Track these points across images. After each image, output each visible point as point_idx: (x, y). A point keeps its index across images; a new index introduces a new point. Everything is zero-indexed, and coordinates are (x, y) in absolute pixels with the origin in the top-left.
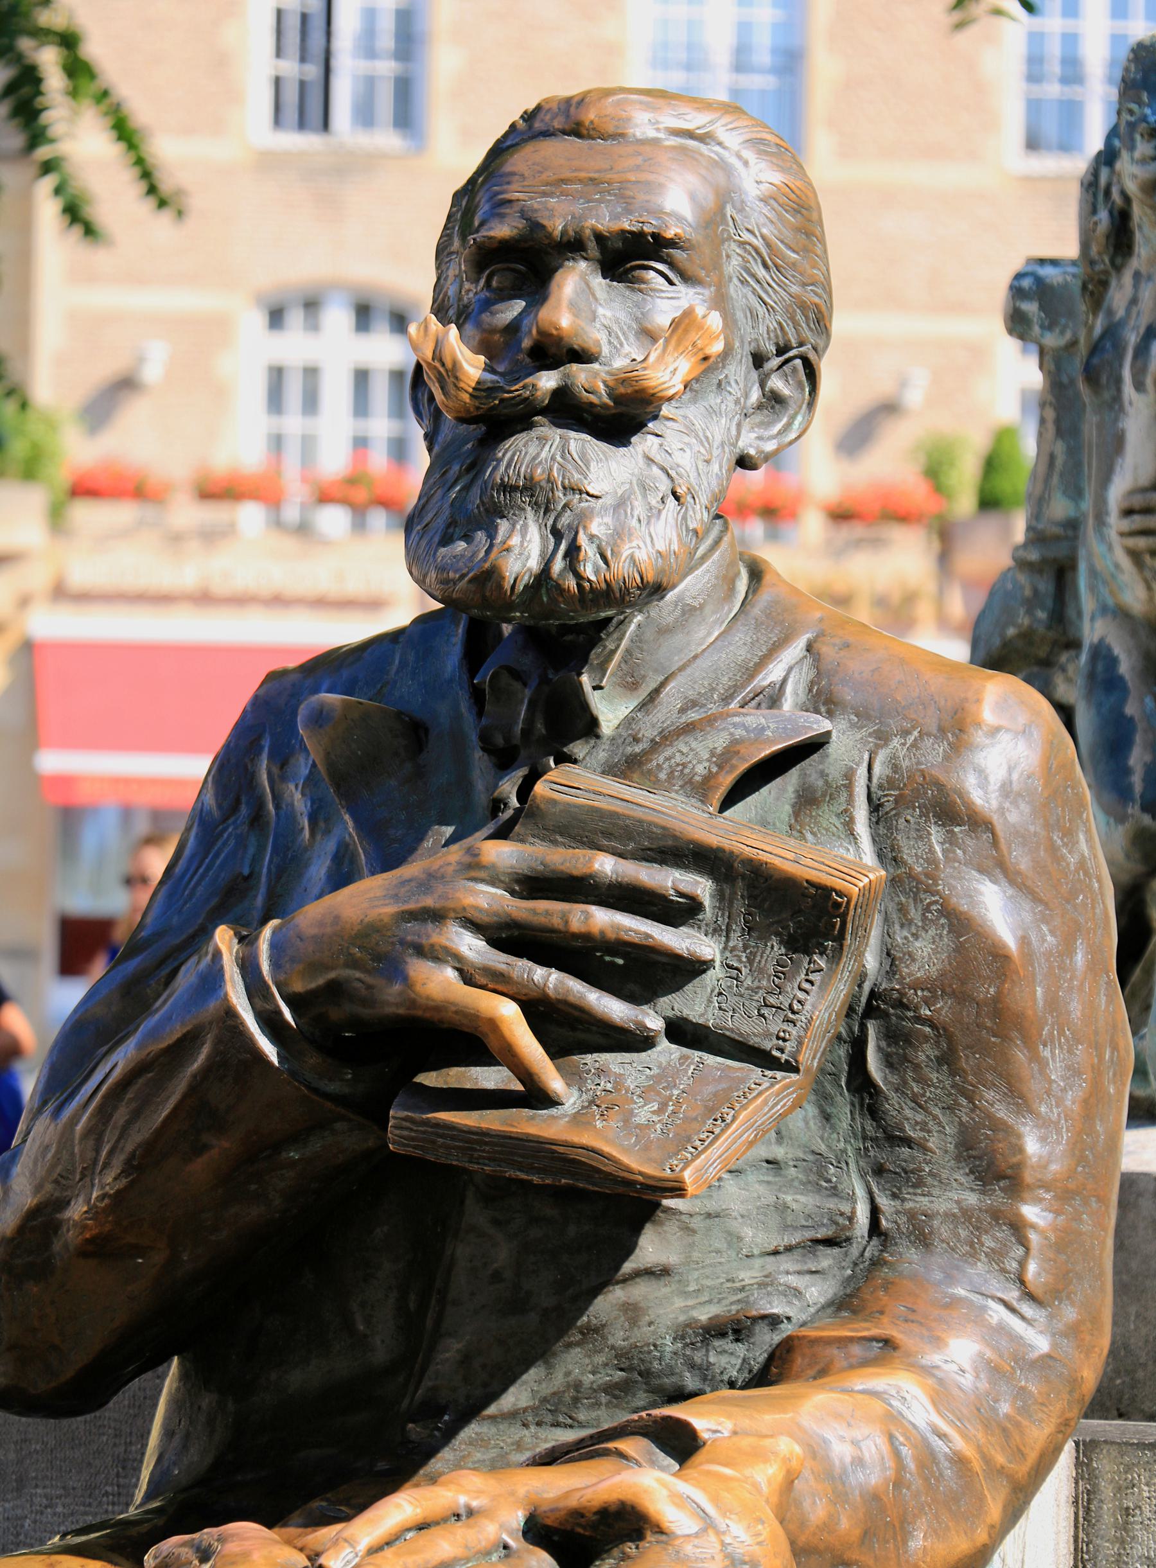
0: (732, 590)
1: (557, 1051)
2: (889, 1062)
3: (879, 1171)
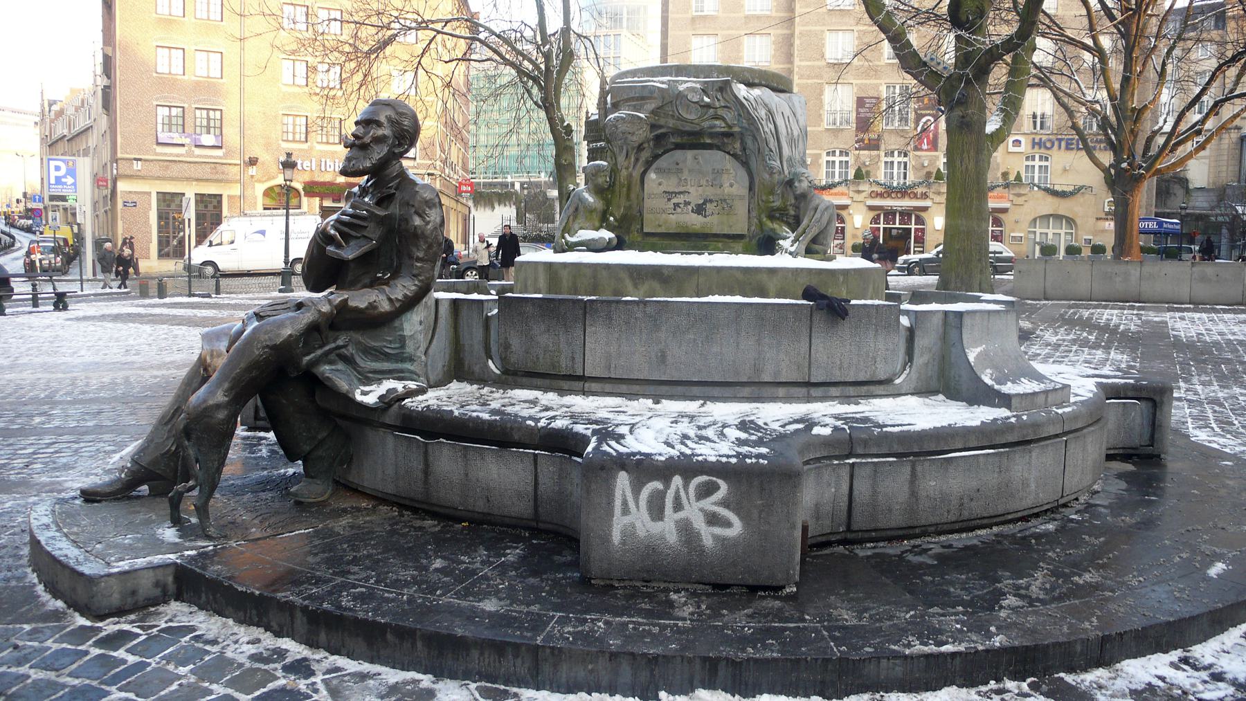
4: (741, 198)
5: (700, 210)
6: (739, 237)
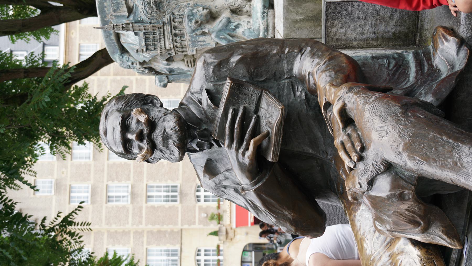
0: (184, 108)
1: (260, 133)
2: (261, 77)
3: (280, 78)
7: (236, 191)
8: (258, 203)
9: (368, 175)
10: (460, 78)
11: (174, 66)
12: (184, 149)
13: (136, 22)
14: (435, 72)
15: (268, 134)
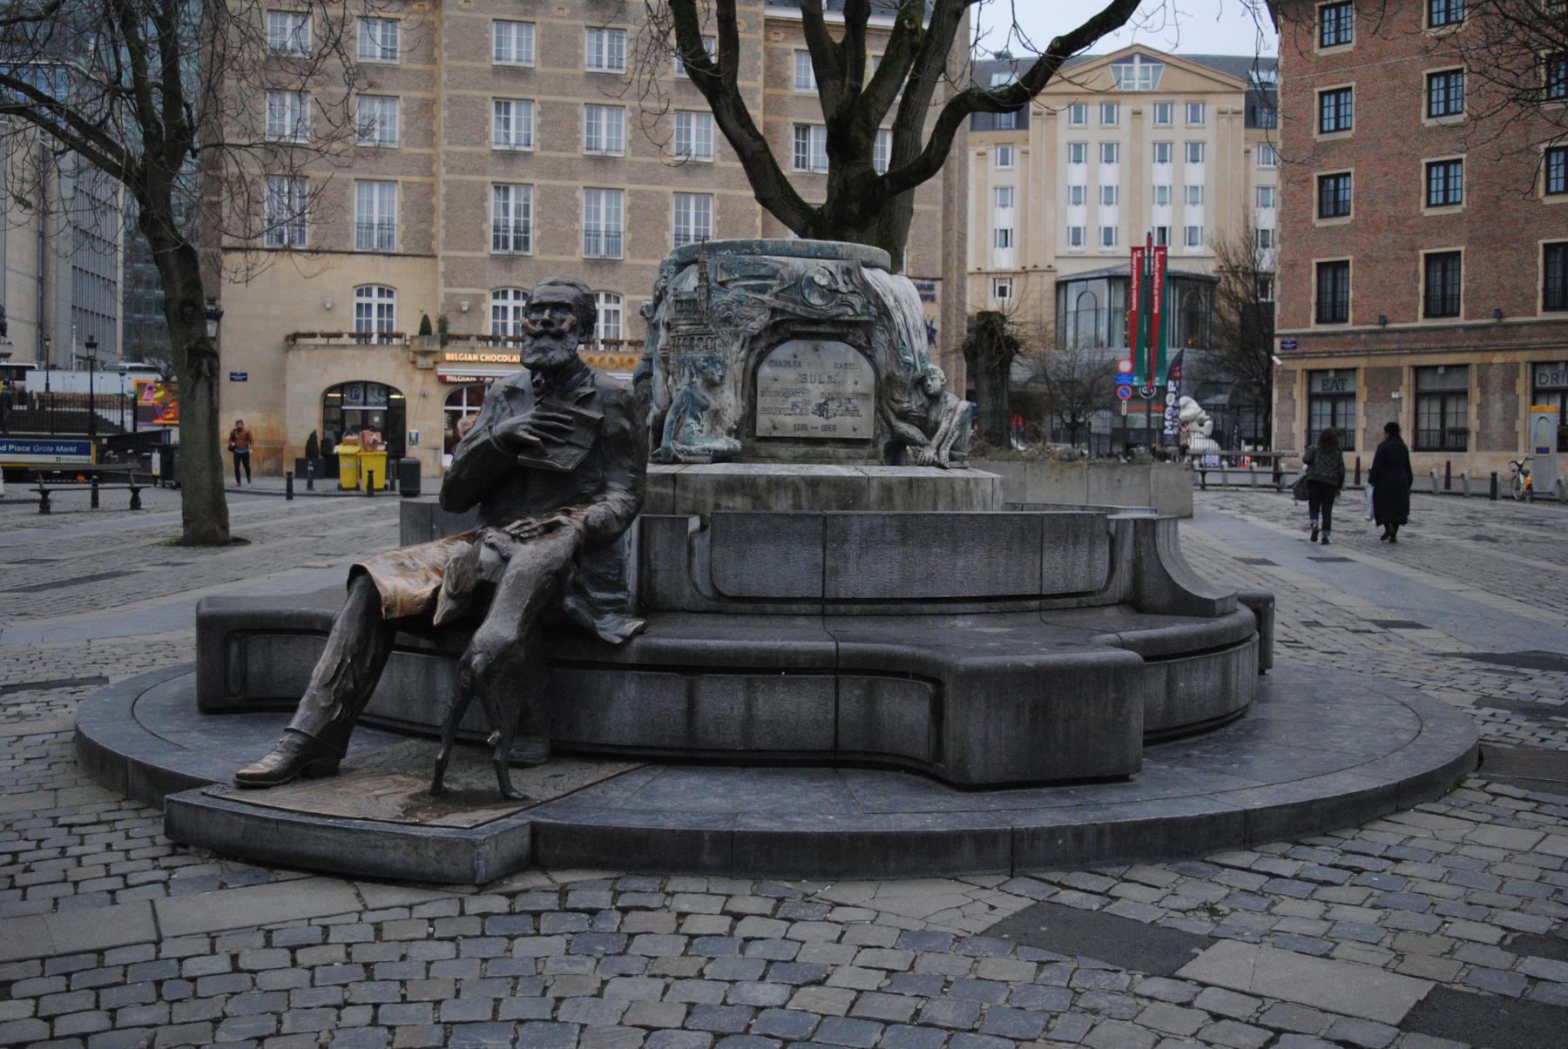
4: (865, 396)
5: (821, 410)
6: (863, 442)
7: (491, 419)
8: (475, 443)
9: (499, 544)
10: (591, 636)
11: (663, 332)
12: (534, 368)
13: (709, 292)
14: (599, 614)
15: (543, 454)
